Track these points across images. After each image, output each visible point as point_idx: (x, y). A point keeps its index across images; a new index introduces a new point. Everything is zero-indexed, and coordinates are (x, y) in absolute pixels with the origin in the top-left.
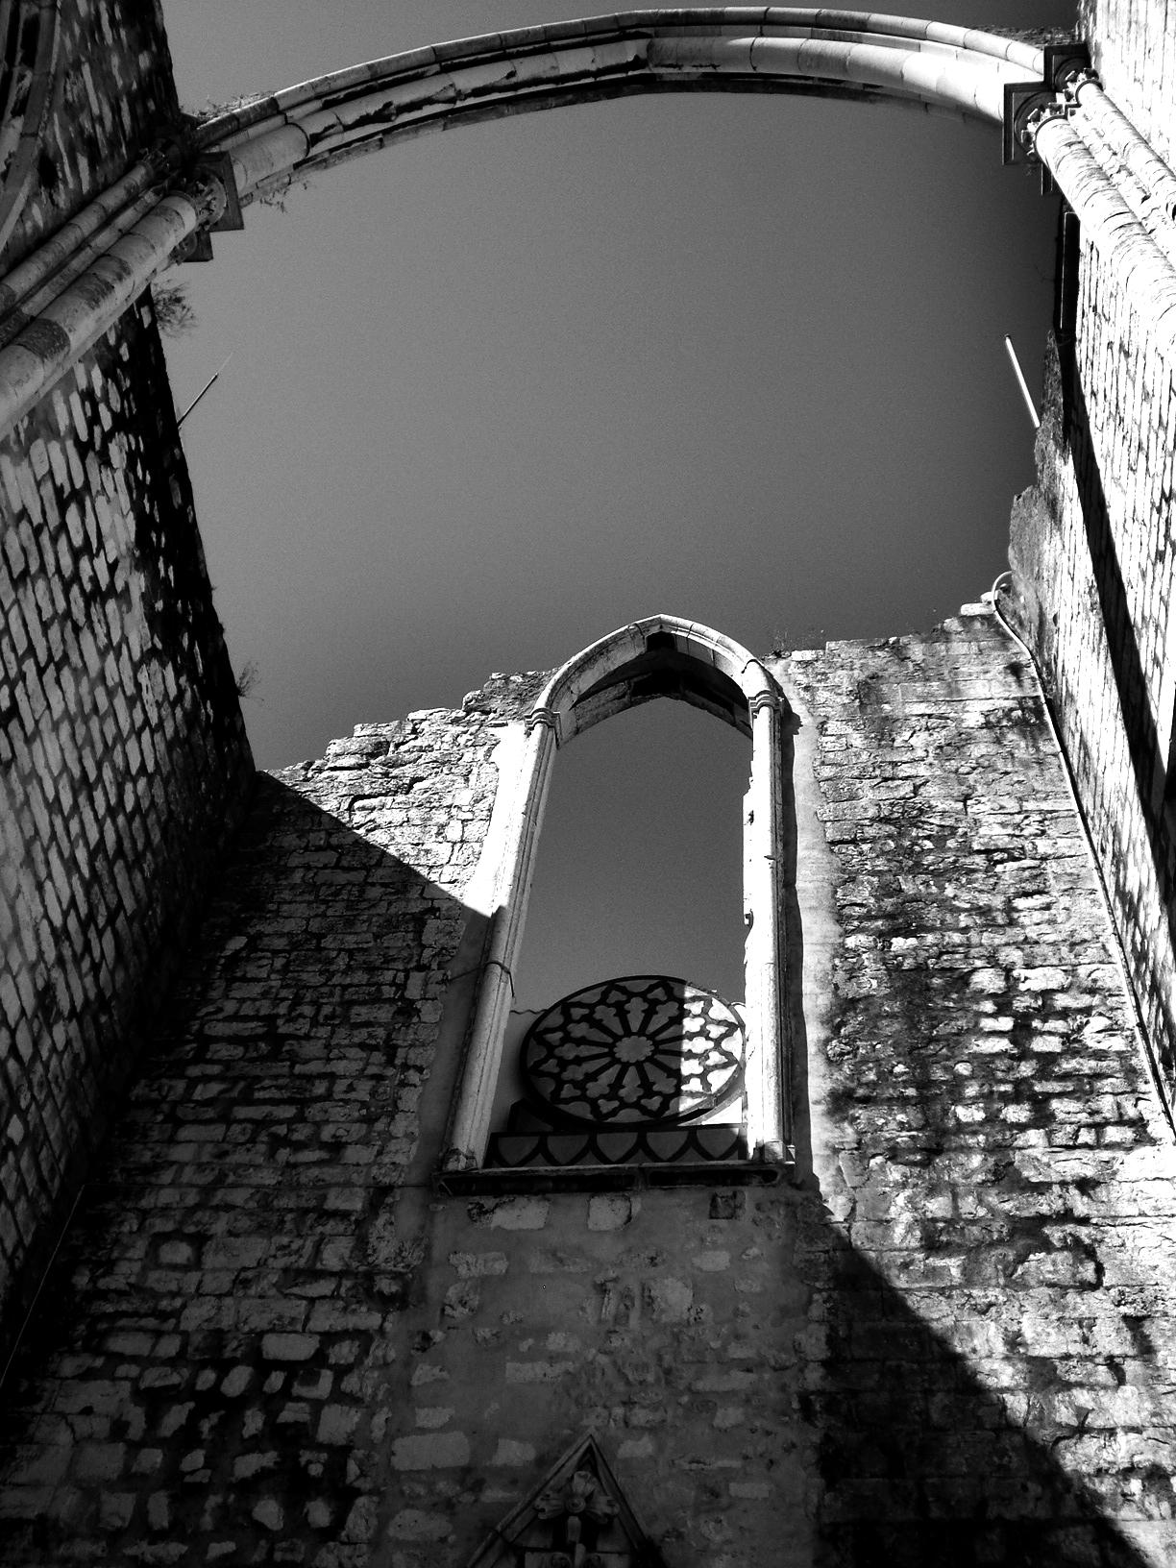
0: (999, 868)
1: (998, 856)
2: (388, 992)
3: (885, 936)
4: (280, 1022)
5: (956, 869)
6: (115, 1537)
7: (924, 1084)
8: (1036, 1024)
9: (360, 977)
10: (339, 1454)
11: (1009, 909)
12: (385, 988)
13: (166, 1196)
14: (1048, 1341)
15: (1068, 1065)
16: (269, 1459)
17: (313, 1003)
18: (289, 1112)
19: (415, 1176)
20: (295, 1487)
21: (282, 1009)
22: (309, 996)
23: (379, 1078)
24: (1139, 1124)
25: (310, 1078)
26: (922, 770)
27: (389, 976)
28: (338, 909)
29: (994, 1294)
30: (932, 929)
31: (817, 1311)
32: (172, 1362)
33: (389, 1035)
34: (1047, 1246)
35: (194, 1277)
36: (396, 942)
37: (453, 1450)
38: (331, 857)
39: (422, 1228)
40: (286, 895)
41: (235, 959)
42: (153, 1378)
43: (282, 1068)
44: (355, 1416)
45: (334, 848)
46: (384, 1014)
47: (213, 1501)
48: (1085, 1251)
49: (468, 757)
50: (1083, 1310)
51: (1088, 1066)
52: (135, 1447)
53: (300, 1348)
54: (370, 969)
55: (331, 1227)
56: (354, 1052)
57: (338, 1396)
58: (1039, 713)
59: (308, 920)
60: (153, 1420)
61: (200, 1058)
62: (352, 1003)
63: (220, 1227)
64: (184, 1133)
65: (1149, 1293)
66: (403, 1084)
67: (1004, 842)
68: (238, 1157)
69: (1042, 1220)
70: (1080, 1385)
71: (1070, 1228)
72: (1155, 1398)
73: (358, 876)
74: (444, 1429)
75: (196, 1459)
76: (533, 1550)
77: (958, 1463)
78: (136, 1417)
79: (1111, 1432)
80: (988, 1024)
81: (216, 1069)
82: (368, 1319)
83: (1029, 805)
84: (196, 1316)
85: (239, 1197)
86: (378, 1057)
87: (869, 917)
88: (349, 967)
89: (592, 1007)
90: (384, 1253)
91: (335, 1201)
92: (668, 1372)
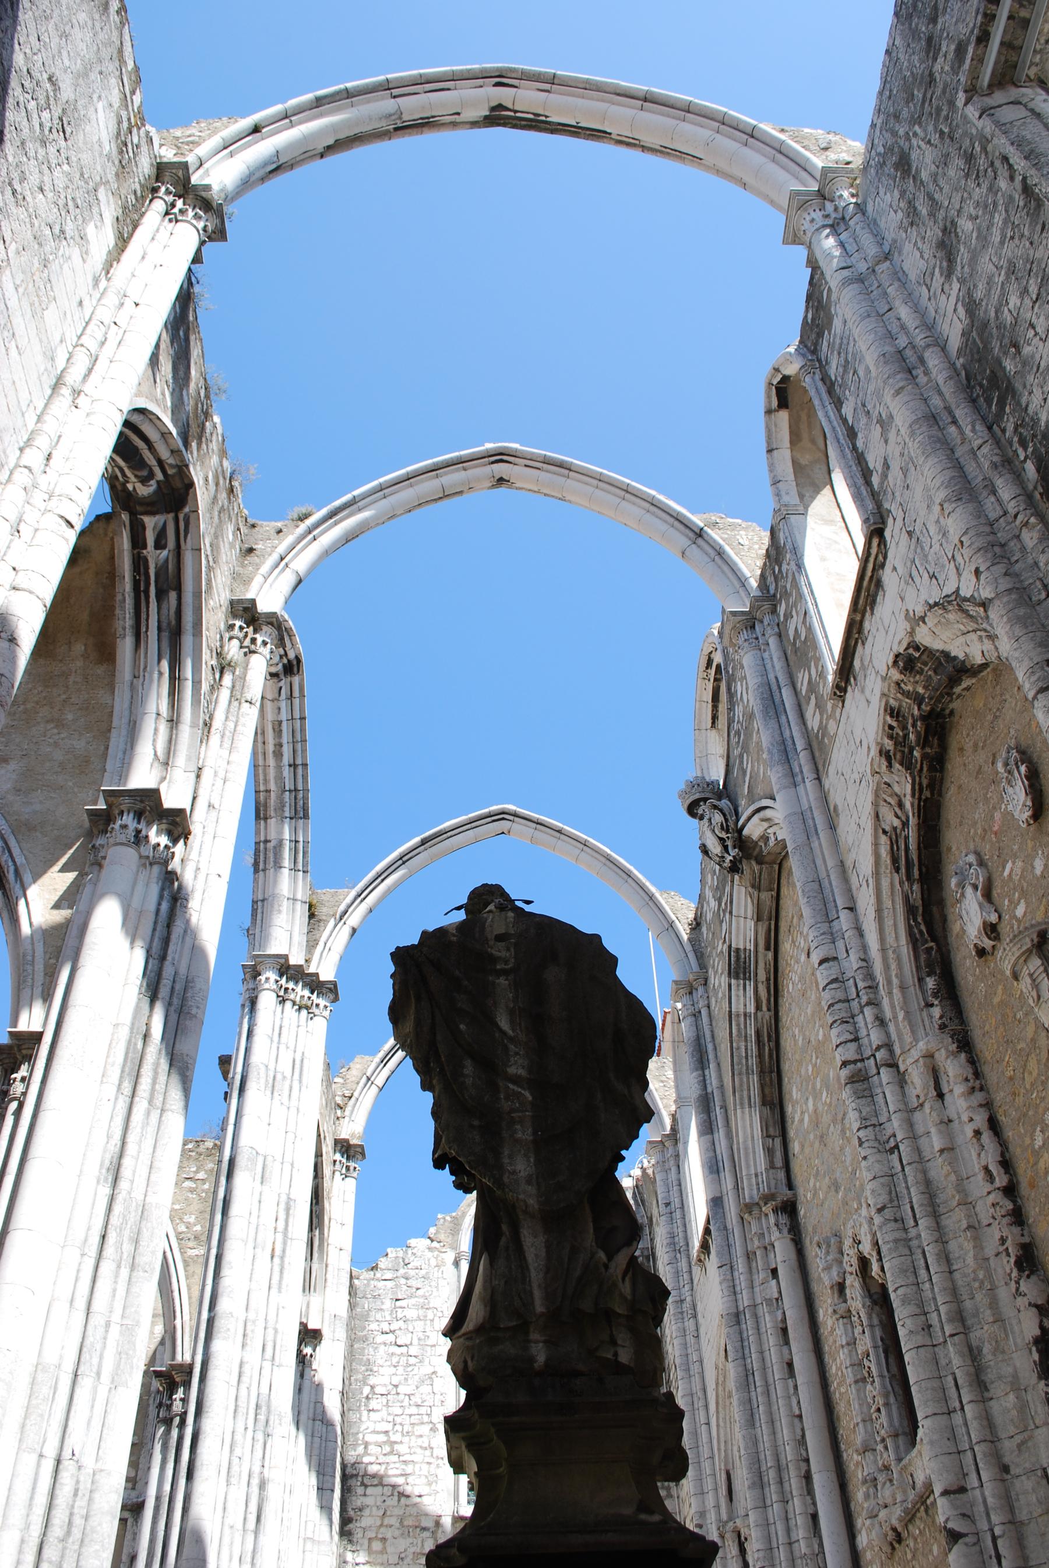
4: (391, 1434)
9: (414, 1410)
17: (401, 1424)
22: (398, 1420)
23: (429, 1463)
27: (423, 1410)
28: (400, 1370)
35: (385, 1556)
36: (425, 1389)
38: (390, 1338)
40: (380, 1362)
43: (395, 1458)
49: (436, 1275)
55: (426, 1534)
56: (419, 1450)
59: (391, 1376)
63: (389, 1535)
85: (393, 1521)
86: (428, 1453)
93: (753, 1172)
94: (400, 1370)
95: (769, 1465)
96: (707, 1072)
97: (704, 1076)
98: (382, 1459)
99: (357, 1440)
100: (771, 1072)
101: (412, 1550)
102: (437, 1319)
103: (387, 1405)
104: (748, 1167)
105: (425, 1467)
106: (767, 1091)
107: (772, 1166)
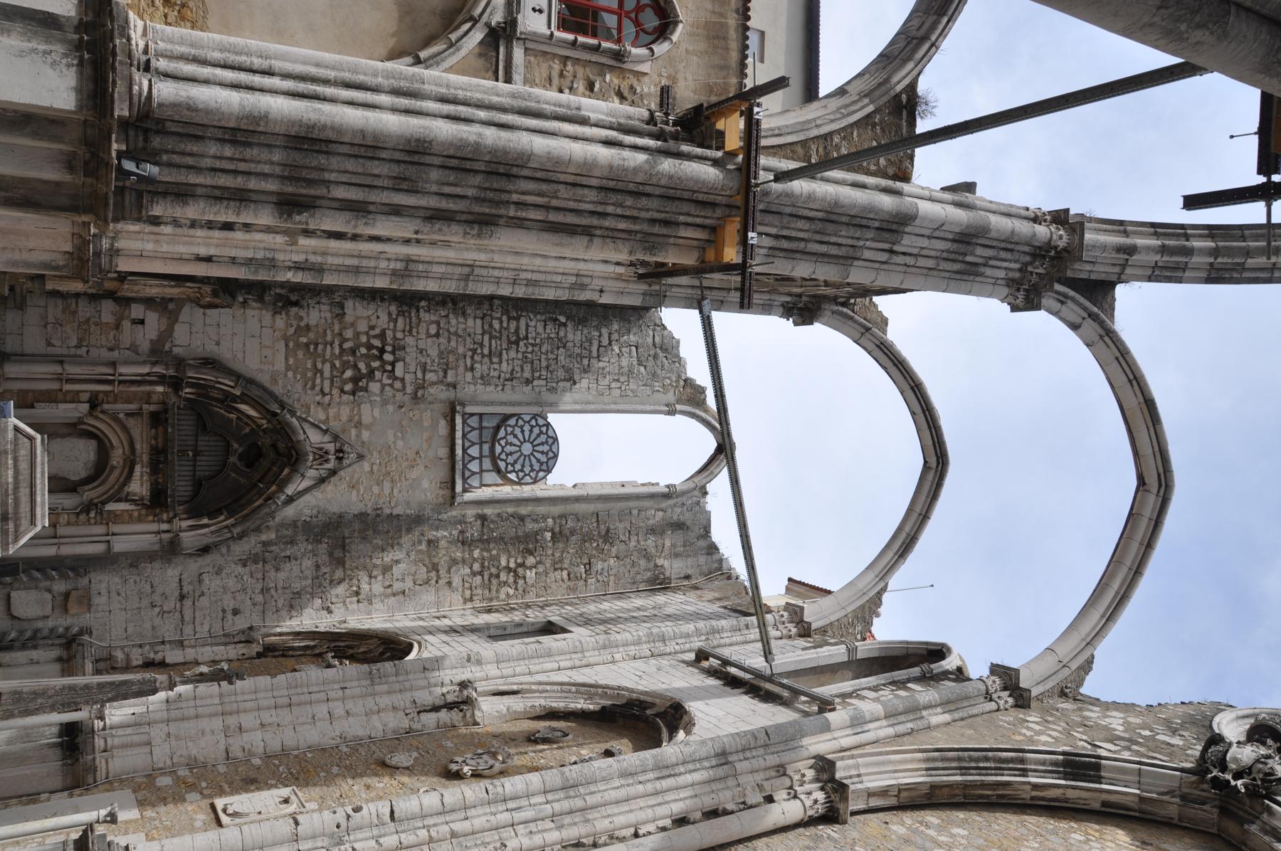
2: (537, 374)
3: (552, 531)
6: (340, 334)
7: (488, 541)
9: (544, 364)
10: (366, 389)
11: (562, 570)
13: (453, 322)
14: (397, 571)
15: (494, 581)
16: (364, 371)
18: (486, 351)
19: (459, 395)
20: (355, 380)
21: (531, 341)
22: (536, 349)
24: (471, 600)
25: (501, 354)
26: (633, 544)
29: (412, 557)
31: (408, 512)
32: (395, 338)
36: (561, 374)
37: (366, 419)
38: (605, 342)
40: (585, 331)
41: (556, 320)
42: (389, 334)
44: (378, 392)
46: (527, 374)
47: (351, 358)
48: (427, 582)
51: (494, 588)
52: (367, 333)
53: (399, 371)
54: (547, 367)
55: (441, 374)
56: (510, 368)
57: (383, 386)
60: (375, 337)
61: (509, 319)
62: (532, 363)
63: (441, 340)
64: (479, 322)
67: (594, 569)
68: (469, 340)
73: (595, 354)
75: (363, 351)
77: (361, 546)
78: (377, 331)
80: (512, 560)
81: (505, 325)
82: (409, 390)
83: (612, 578)
84: (410, 341)
85: (453, 344)
90: (432, 390)
91: (450, 373)
93: (862, 771)
94: (577, 350)
95: (587, 798)
96: (939, 710)
97: (936, 706)
98: (505, 333)
99: (522, 310)
100: (965, 797)
101: (429, 361)
102: (619, 385)
103: (549, 338)
104: (867, 765)
105: (496, 374)
106: (945, 791)
107: (871, 794)
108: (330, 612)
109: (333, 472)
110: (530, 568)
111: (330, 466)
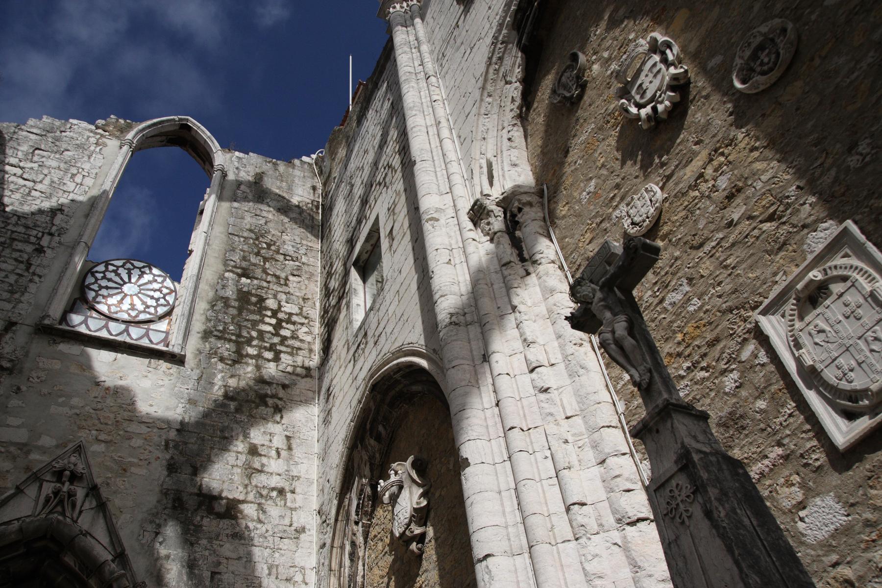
0: (287, 262)
1: (288, 258)
3: (240, 276)
5: (272, 258)
7: (239, 336)
8: (284, 324)
9: (21, 229)
11: (287, 279)
12: (32, 238)
15: (290, 342)
27: (34, 233)
30: (257, 279)
33: (29, 259)
34: (266, 405)
38: (19, 171)
39: (27, 343)
45: (22, 168)
46: (29, 248)
49: (92, 148)
50: (272, 430)
51: (297, 344)
54: (27, 227)
58: (318, 208)
62: (15, 239)
65: (296, 429)
66: (31, 281)
67: (291, 253)
69: (266, 395)
70: (265, 456)
71: (276, 400)
72: (288, 465)
74: (18, 427)
76: (47, 481)
79: (272, 474)
80: (267, 320)
86: (22, 266)
87: (235, 267)
88: (17, 224)
89: (118, 267)
92: (117, 422)
108: (302, 530)
109: (93, 490)
110: (280, 306)
111: (80, 493)
